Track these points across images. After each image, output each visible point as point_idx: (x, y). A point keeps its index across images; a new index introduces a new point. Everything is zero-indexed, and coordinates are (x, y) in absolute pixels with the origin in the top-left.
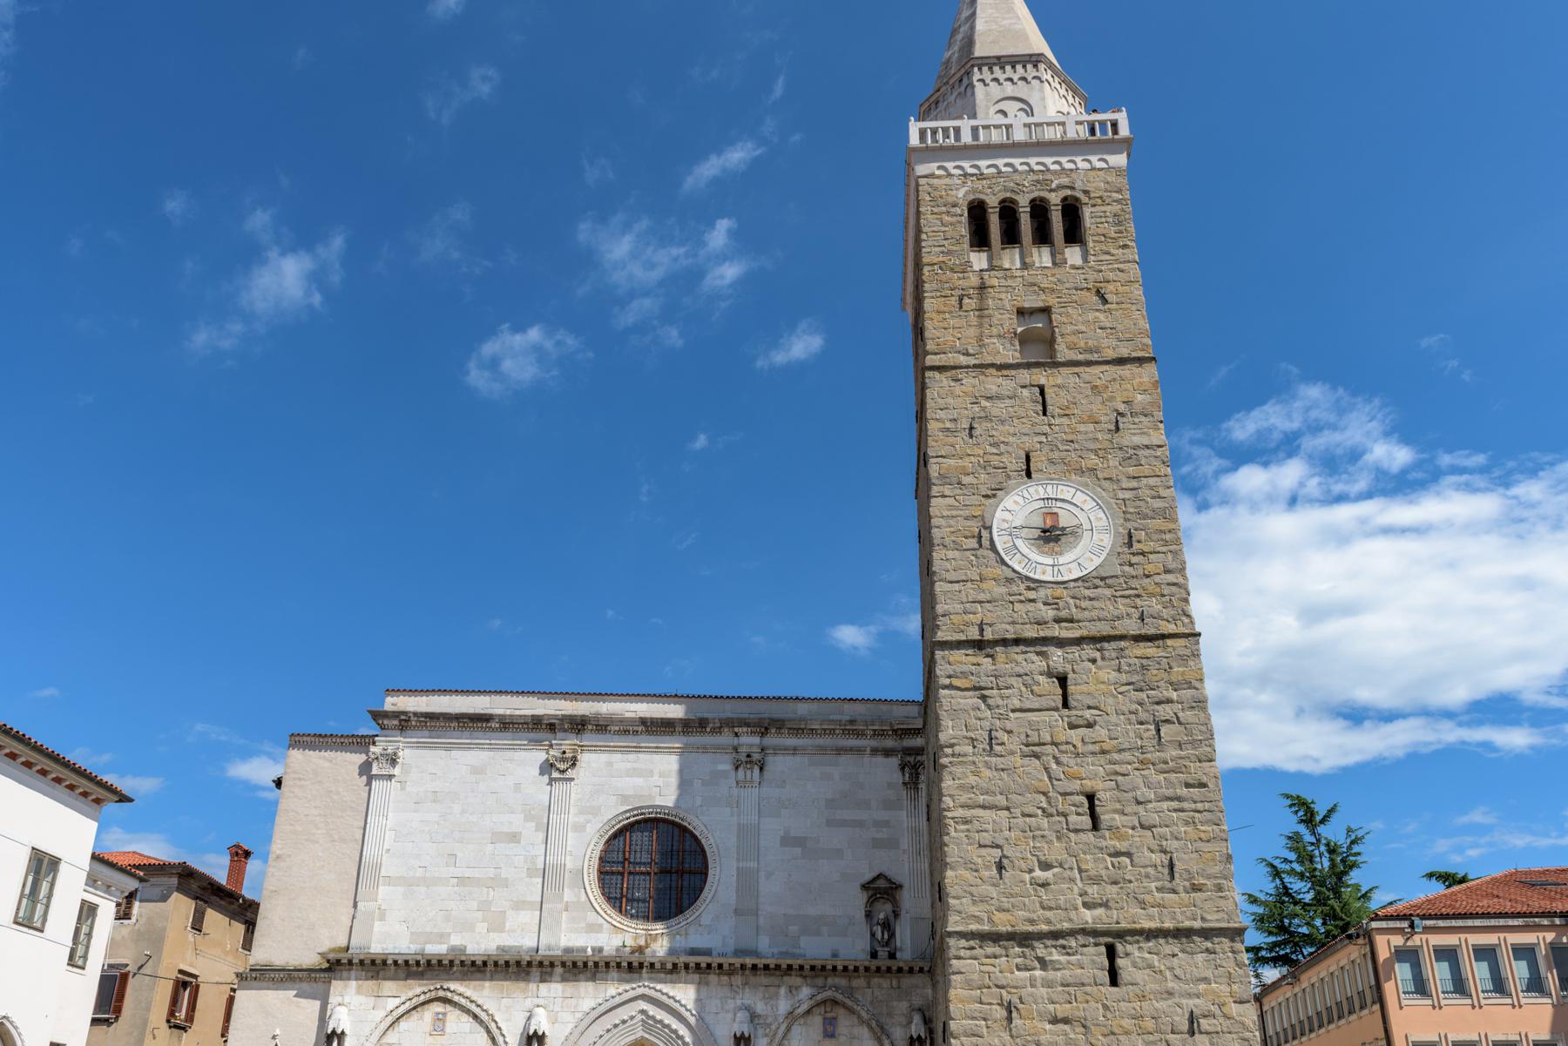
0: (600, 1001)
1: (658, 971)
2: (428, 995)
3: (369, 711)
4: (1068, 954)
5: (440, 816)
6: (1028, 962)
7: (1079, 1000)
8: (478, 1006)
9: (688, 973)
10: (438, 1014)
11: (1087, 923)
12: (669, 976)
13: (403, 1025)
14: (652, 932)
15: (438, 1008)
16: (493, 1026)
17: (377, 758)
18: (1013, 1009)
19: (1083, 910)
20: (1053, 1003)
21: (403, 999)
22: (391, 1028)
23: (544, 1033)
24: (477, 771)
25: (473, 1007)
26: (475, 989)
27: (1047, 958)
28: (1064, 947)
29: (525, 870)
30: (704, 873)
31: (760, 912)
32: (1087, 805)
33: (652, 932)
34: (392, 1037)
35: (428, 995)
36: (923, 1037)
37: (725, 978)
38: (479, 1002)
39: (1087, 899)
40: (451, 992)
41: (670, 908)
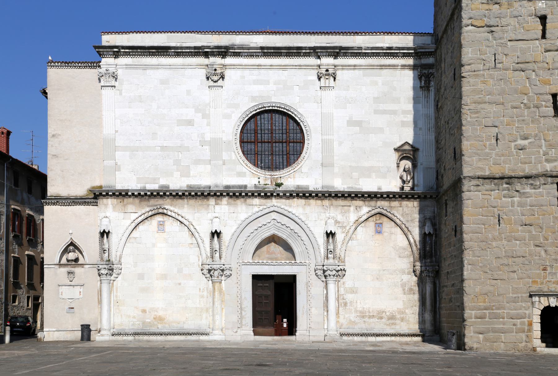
1: (281, 197)
3: (93, 46)
4: (534, 188)
5: (145, 110)
6: (510, 193)
7: (539, 214)
8: (182, 217)
9: (297, 199)
10: (160, 221)
11: (547, 171)
12: (288, 201)
13: (141, 227)
14: (275, 177)
15: (159, 218)
16: (191, 228)
17: (103, 76)
18: (500, 219)
19: (545, 163)
20: (524, 215)
21: (140, 214)
22: (135, 229)
23: (220, 231)
24: (164, 82)
26: (179, 208)
27: (522, 191)
28: (532, 184)
29: (199, 141)
30: (302, 142)
31: (335, 165)
32: (552, 101)
33: (275, 177)
34: (135, 234)
36: (432, 233)
39: (547, 157)
41: (283, 163)
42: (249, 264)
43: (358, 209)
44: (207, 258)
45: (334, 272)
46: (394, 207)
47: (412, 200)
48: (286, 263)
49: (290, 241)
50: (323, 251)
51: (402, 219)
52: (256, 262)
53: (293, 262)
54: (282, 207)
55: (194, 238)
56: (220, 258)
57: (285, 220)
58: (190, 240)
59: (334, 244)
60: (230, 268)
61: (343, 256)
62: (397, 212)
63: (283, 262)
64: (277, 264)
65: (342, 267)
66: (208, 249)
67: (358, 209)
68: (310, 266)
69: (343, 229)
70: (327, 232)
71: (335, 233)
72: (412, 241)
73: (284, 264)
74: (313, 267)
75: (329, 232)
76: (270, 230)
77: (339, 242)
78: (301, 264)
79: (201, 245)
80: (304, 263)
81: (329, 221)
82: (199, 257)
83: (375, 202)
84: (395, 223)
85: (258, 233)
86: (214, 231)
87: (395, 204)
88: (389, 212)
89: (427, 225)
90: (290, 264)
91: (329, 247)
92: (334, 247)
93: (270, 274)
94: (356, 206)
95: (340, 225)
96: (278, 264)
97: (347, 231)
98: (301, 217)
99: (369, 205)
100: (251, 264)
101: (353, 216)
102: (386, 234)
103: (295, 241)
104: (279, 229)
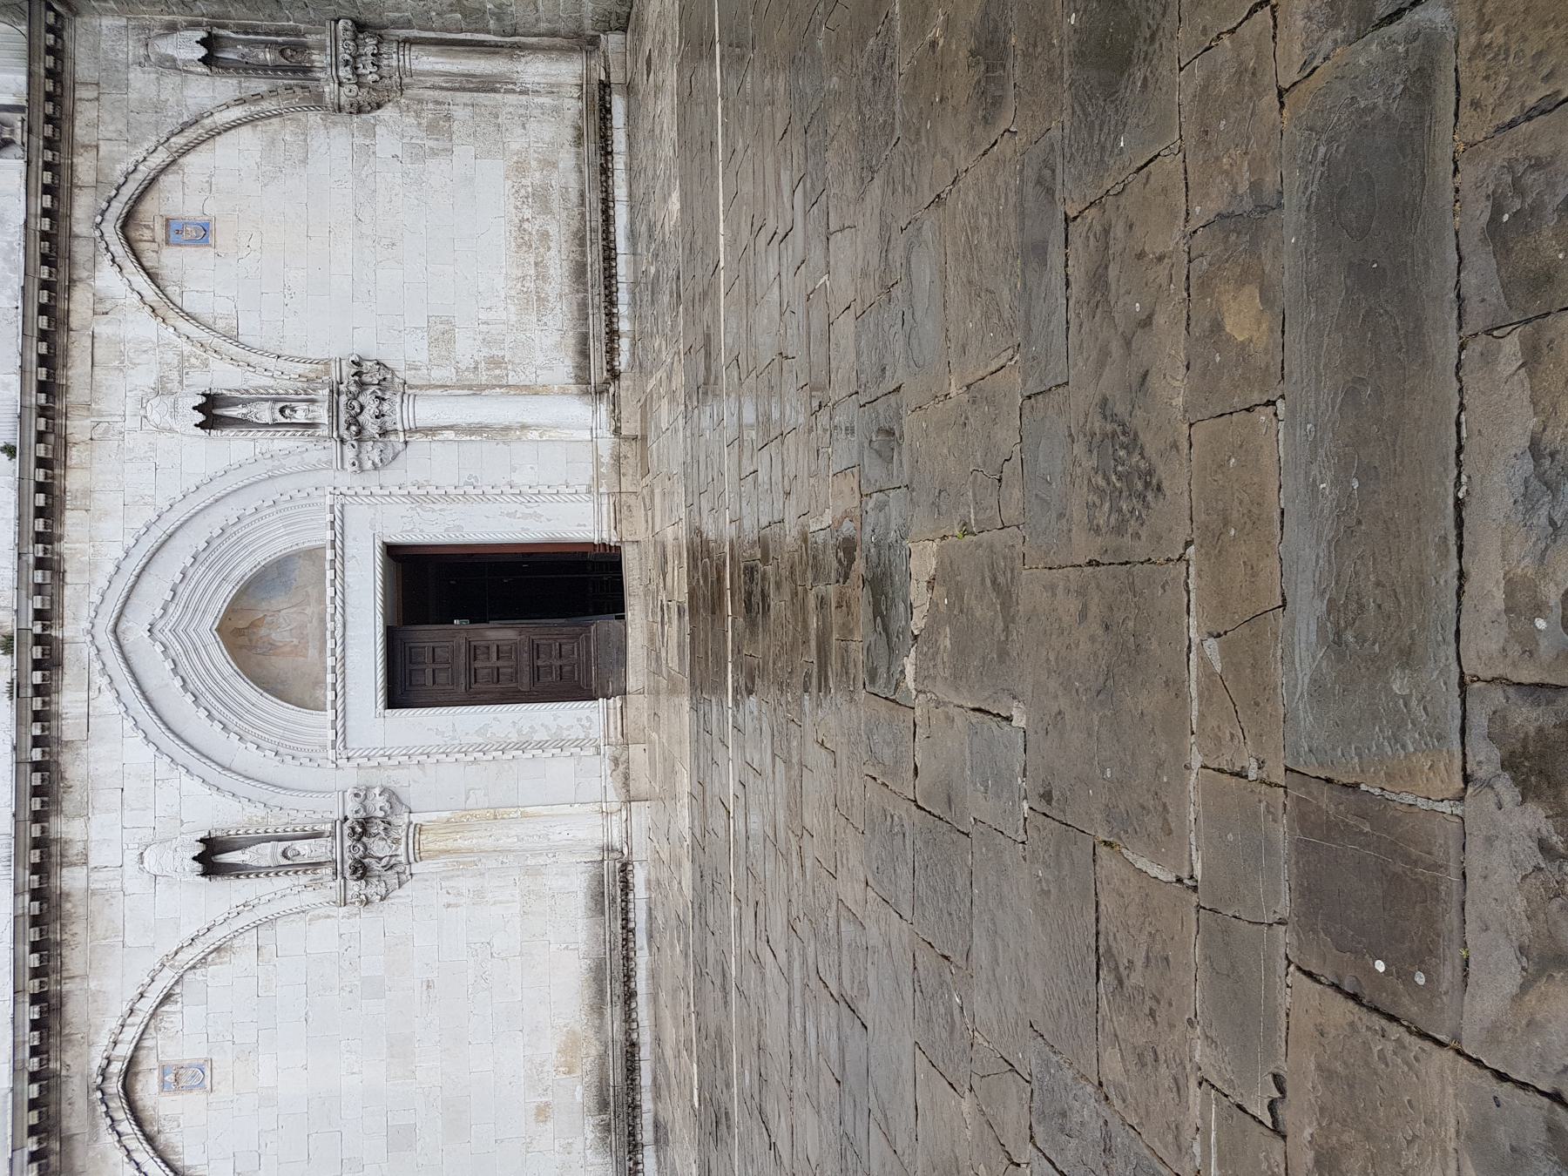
0: (129, 724)
1: (56, 600)
2: (120, 1115)
8: (142, 995)
9: (60, 538)
10: (163, 1083)
12: (68, 578)
15: (148, 1089)
23: (202, 841)
25: (146, 1006)
35: (120, 1115)
37: (74, 455)
38: (135, 993)
40: (108, 1064)
42: (339, 724)
43: (108, 305)
44: (317, 884)
45: (367, 398)
46: (98, 170)
47: (67, 103)
48: (333, 581)
49: (245, 568)
50: (283, 442)
51: (150, 144)
52: (330, 695)
53: (329, 554)
54: (96, 599)
55: (237, 943)
56: (316, 835)
57: (156, 589)
58: (244, 958)
59: (253, 401)
60: (356, 795)
61: (302, 368)
62: (119, 161)
63: (330, 592)
64: (338, 616)
65: (347, 370)
66: (283, 882)
67: (108, 305)
68: (344, 490)
69: (192, 366)
70: (201, 425)
71: (203, 395)
72: (237, 113)
73: (338, 587)
74: (347, 479)
75: (200, 417)
76: (199, 644)
77: (246, 380)
78: (338, 525)
79: (262, 912)
80: (332, 512)
81: (155, 417)
82: (319, 918)
83: (76, 242)
84: (163, 170)
85: (209, 689)
86: (198, 866)
87: (84, 167)
88: (118, 189)
89: (170, 51)
90: (338, 565)
91: (265, 413)
92: (267, 400)
93: (380, 640)
94: (95, 313)
95: (175, 375)
96: (339, 608)
97: (199, 352)
98: (139, 525)
99: (89, 265)
100: (340, 717)
101: (138, 327)
102: (212, 209)
103: (245, 547)
104: (195, 610)
